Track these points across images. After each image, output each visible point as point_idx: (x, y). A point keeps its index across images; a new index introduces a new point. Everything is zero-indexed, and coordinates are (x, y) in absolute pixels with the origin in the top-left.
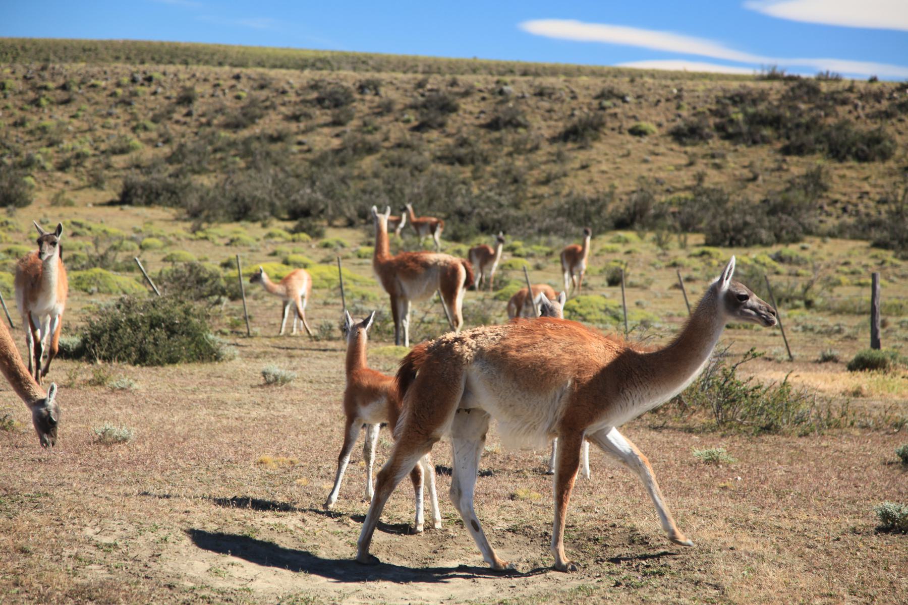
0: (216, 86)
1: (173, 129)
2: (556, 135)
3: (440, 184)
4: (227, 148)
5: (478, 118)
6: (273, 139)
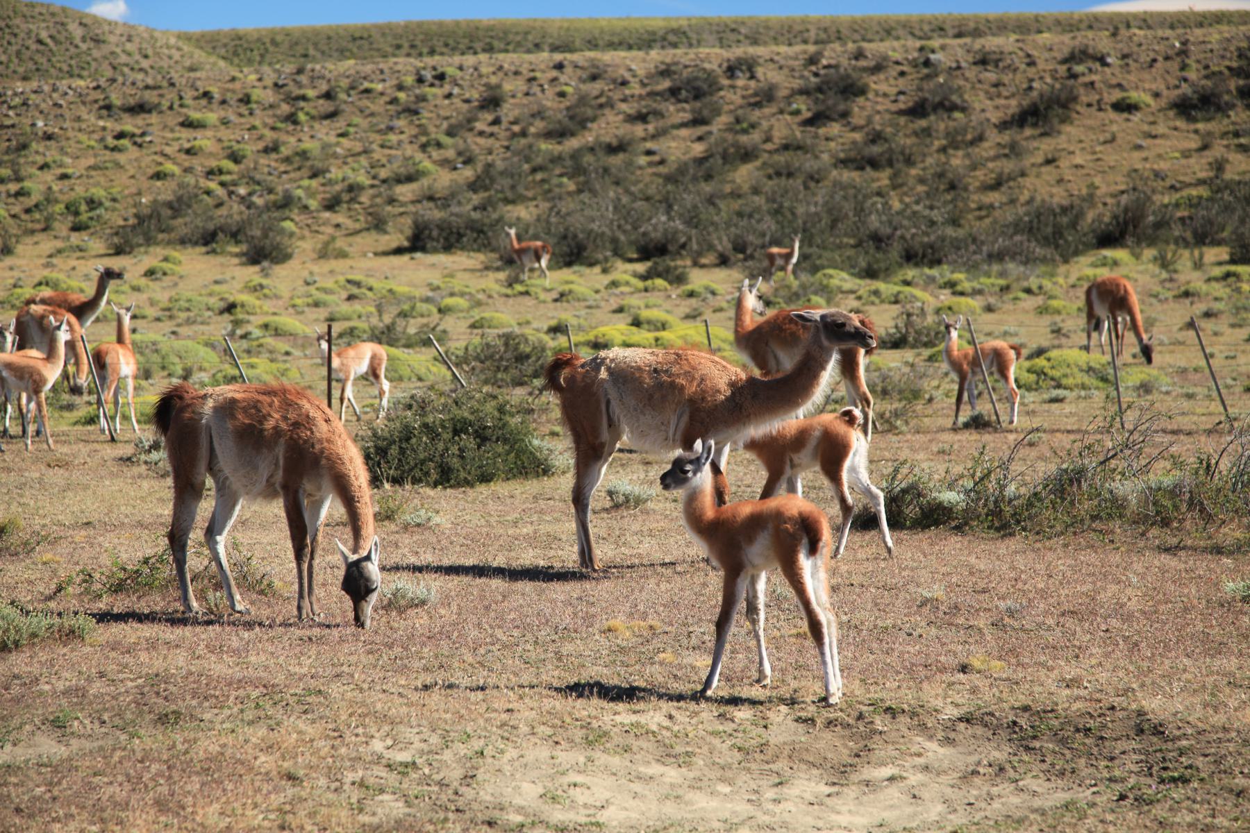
1: (477, 144)
2: (1008, 118)
3: (845, 198)
4: (551, 166)
5: (895, 101)
6: (612, 149)
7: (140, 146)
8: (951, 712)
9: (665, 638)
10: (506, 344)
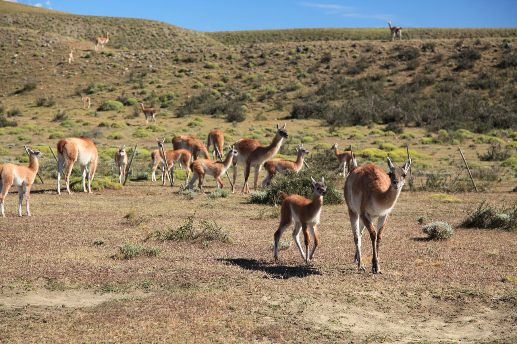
0: (342, 51)
1: (320, 76)
3: (470, 101)
4: (349, 85)
5: (492, 62)
6: (374, 79)
7: (188, 75)
8: (496, 297)
10: (327, 154)
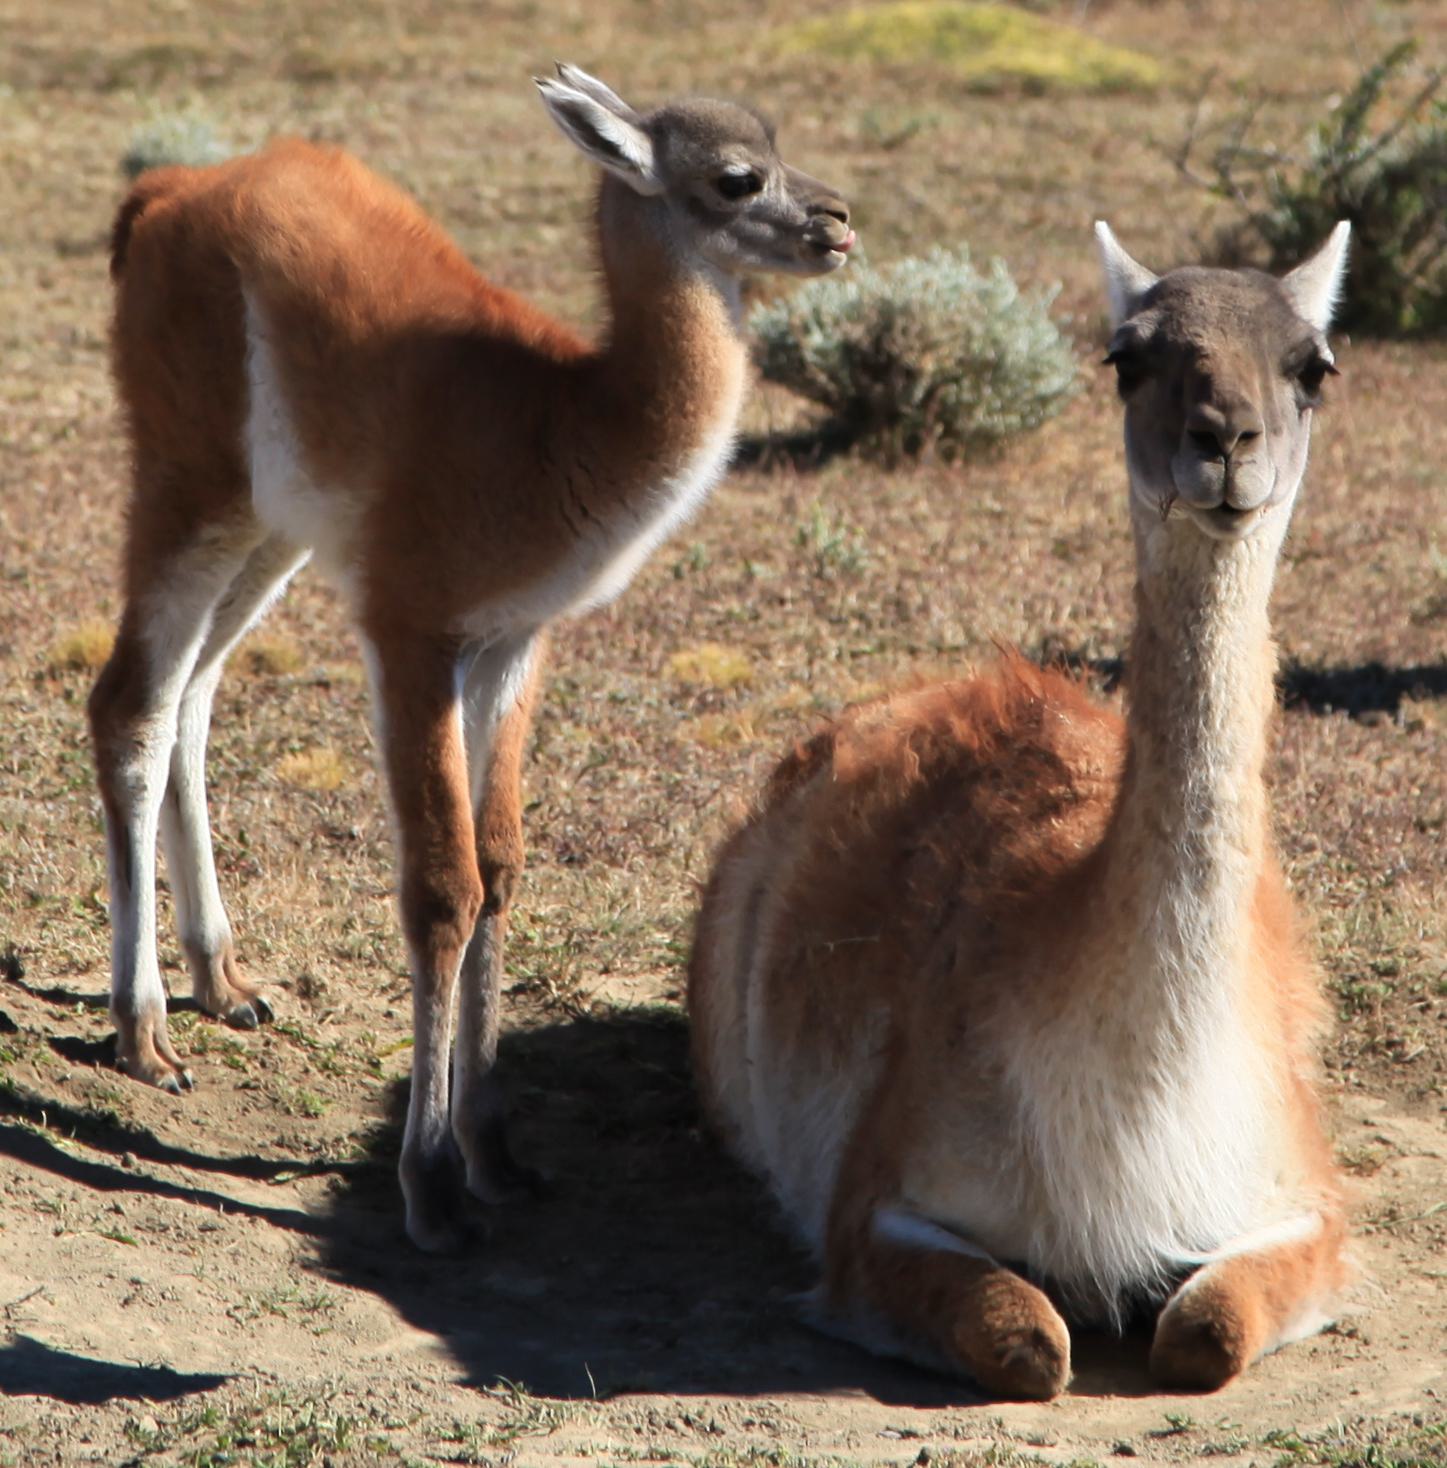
9: (315, 703)
